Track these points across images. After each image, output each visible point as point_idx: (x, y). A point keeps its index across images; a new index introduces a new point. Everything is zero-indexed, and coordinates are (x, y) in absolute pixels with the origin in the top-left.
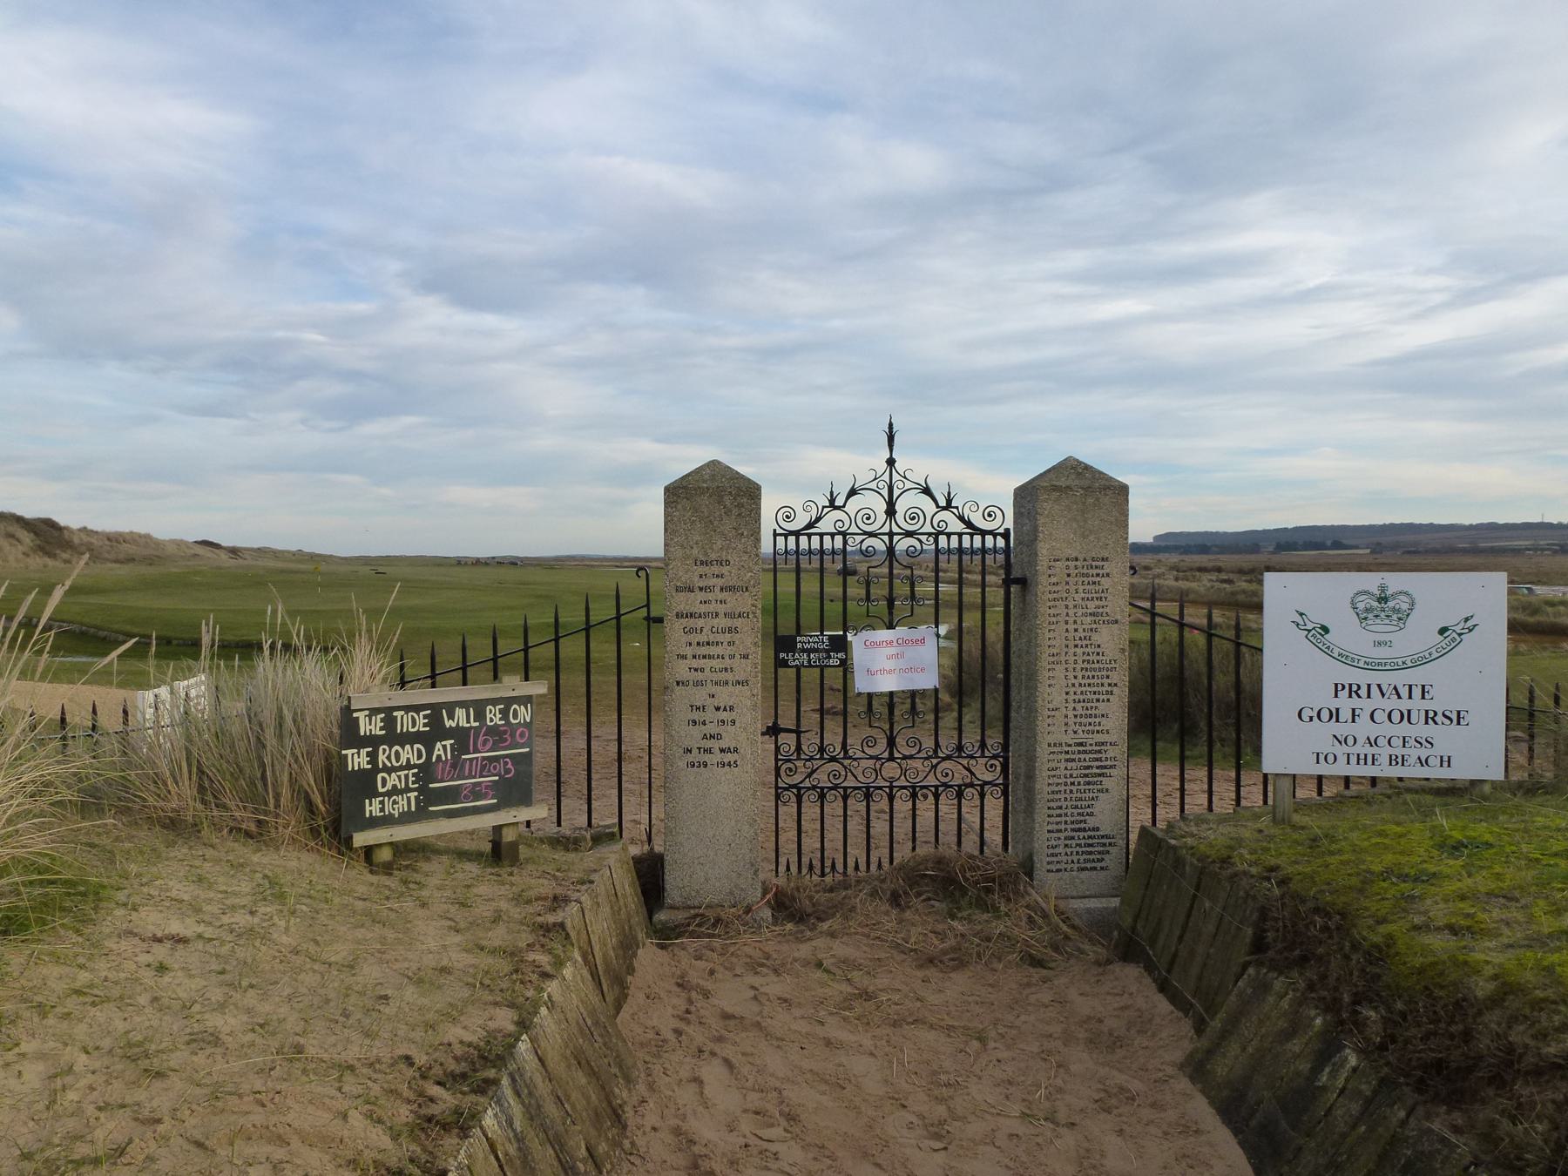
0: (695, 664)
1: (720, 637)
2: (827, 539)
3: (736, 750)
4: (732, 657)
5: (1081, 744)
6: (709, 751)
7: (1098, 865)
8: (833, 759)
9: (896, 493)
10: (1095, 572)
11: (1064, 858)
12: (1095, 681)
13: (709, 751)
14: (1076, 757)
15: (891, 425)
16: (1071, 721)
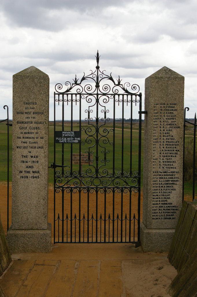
0: (24, 140)
1: (33, 131)
2: (74, 96)
3: (38, 172)
4: (37, 138)
5: (165, 172)
6: (29, 172)
7: (172, 217)
8: (76, 177)
9: (100, 79)
10: (171, 109)
11: (159, 214)
12: (171, 149)
13: (29, 172)
14: (164, 177)
15: (98, 54)
16: (162, 164)
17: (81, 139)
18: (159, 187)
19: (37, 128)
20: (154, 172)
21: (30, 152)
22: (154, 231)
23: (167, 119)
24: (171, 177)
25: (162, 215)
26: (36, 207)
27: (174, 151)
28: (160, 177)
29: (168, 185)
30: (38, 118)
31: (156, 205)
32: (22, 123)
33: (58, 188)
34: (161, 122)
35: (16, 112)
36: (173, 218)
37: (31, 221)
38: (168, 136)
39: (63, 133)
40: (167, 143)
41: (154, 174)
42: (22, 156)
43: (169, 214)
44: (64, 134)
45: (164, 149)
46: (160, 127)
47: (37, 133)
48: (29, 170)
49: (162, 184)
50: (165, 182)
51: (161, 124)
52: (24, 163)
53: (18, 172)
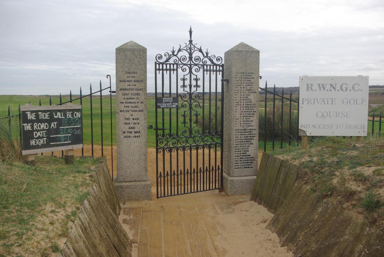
0: (126, 105)
1: (134, 97)
2: (172, 65)
3: (139, 132)
4: (138, 103)
5: (245, 130)
6: (131, 132)
7: (250, 166)
8: (174, 138)
9: (192, 51)
10: (249, 77)
11: (240, 164)
12: (249, 110)
13: (131, 132)
14: (243, 133)
15: (191, 29)
16: (242, 123)
17: (178, 104)
18: (240, 142)
19: (137, 94)
20: (236, 130)
21: (132, 115)
22: (236, 178)
23: (246, 85)
24: (249, 133)
25: (242, 165)
26: (138, 162)
27: (251, 112)
28: (241, 133)
29: (247, 140)
30: (138, 85)
31: (238, 157)
32: (125, 89)
33: (160, 149)
34: (241, 88)
35: (119, 80)
36: (251, 167)
37: (134, 174)
38: (247, 100)
39: (164, 99)
40: (246, 106)
41: (236, 131)
42: (125, 118)
43: (248, 164)
44: (164, 100)
45: (243, 111)
46: (241, 92)
47: (138, 98)
48: (131, 130)
49: (242, 139)
50: (244, 138)
51: (241, 90)
52: (127, 125)
53: (122, 132)
